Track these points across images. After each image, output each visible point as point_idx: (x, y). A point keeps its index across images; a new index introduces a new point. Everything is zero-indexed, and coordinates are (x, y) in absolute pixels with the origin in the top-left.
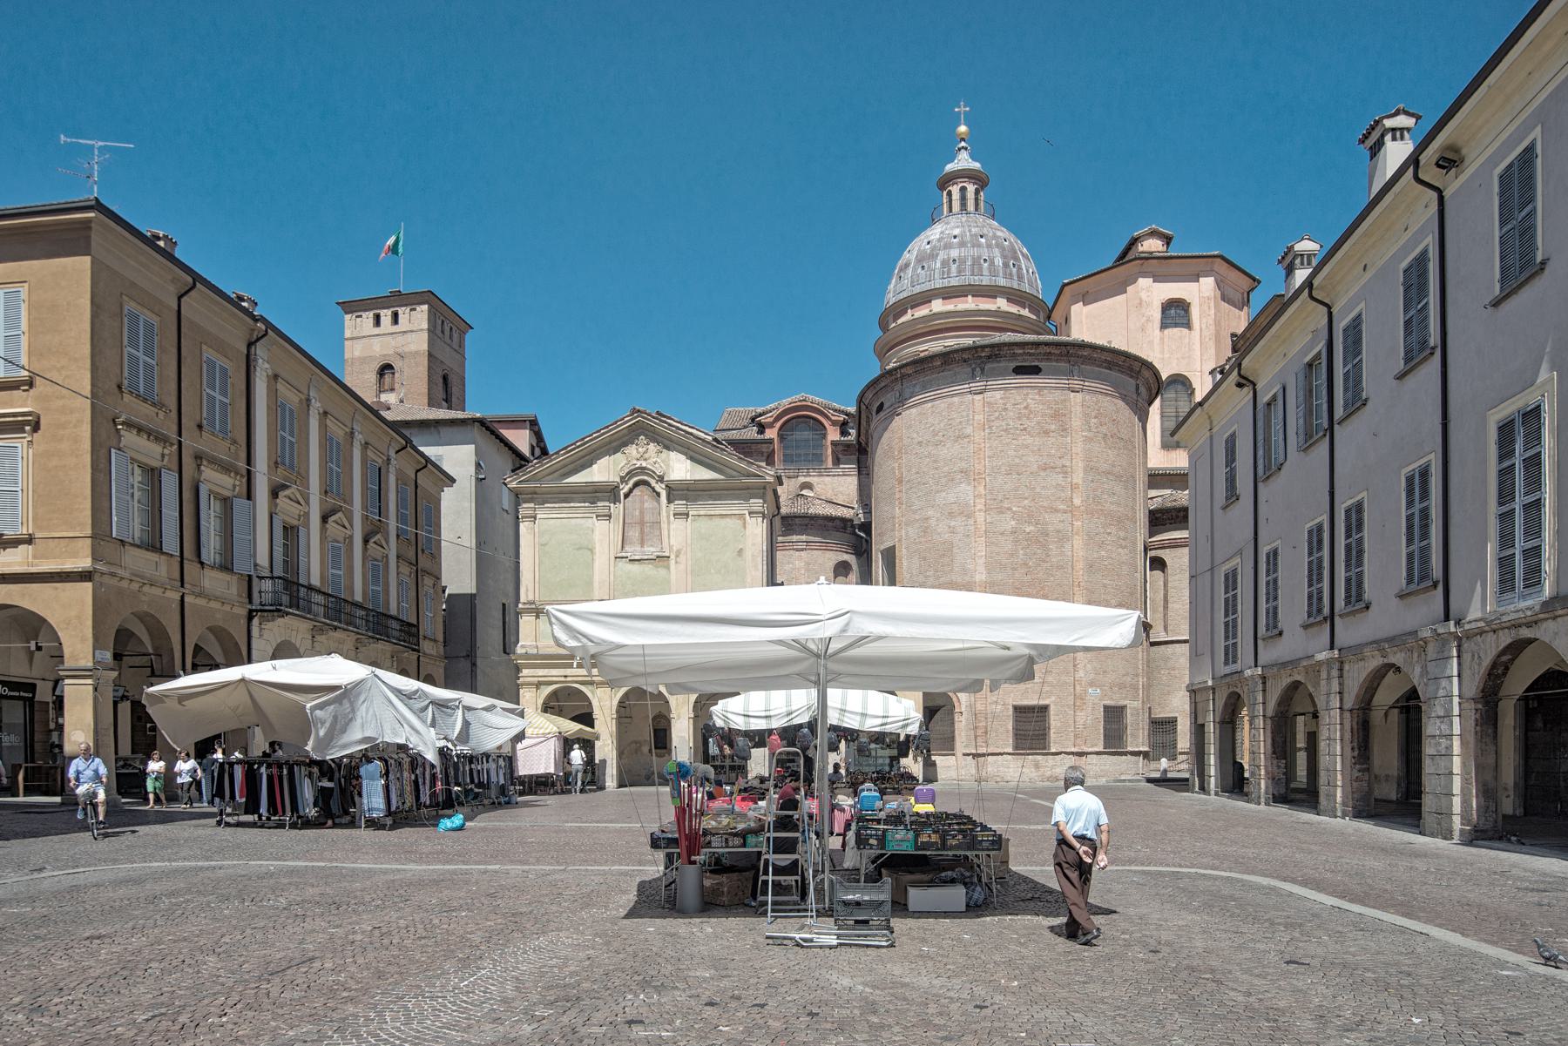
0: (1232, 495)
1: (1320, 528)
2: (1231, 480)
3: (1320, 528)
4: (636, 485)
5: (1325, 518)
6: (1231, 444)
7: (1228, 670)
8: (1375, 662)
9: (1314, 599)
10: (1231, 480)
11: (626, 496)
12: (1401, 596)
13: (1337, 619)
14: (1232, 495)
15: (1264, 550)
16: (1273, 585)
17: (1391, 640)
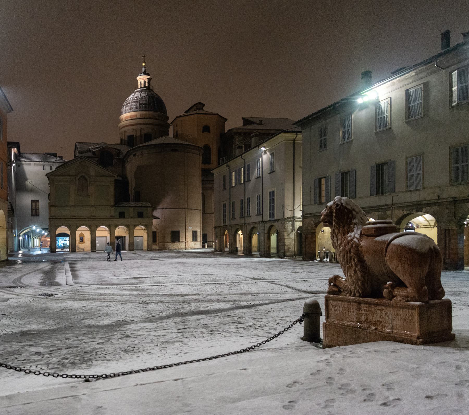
0: (225, 188)
1: (243, 200)
2: (224, 185)
3: (243, 200)
4: (81, 177)
5: (244, 198)
6: (224, 177)
7: (224, 224)
8: (252, 226)
9: (242, 213)
10: (224, 185)
11: (79, 179)
12: (256, 215)
13: (246, 218)
14: (225, 188)
15: (232, 201)
16: (233, 209)
17: (255, 223)
